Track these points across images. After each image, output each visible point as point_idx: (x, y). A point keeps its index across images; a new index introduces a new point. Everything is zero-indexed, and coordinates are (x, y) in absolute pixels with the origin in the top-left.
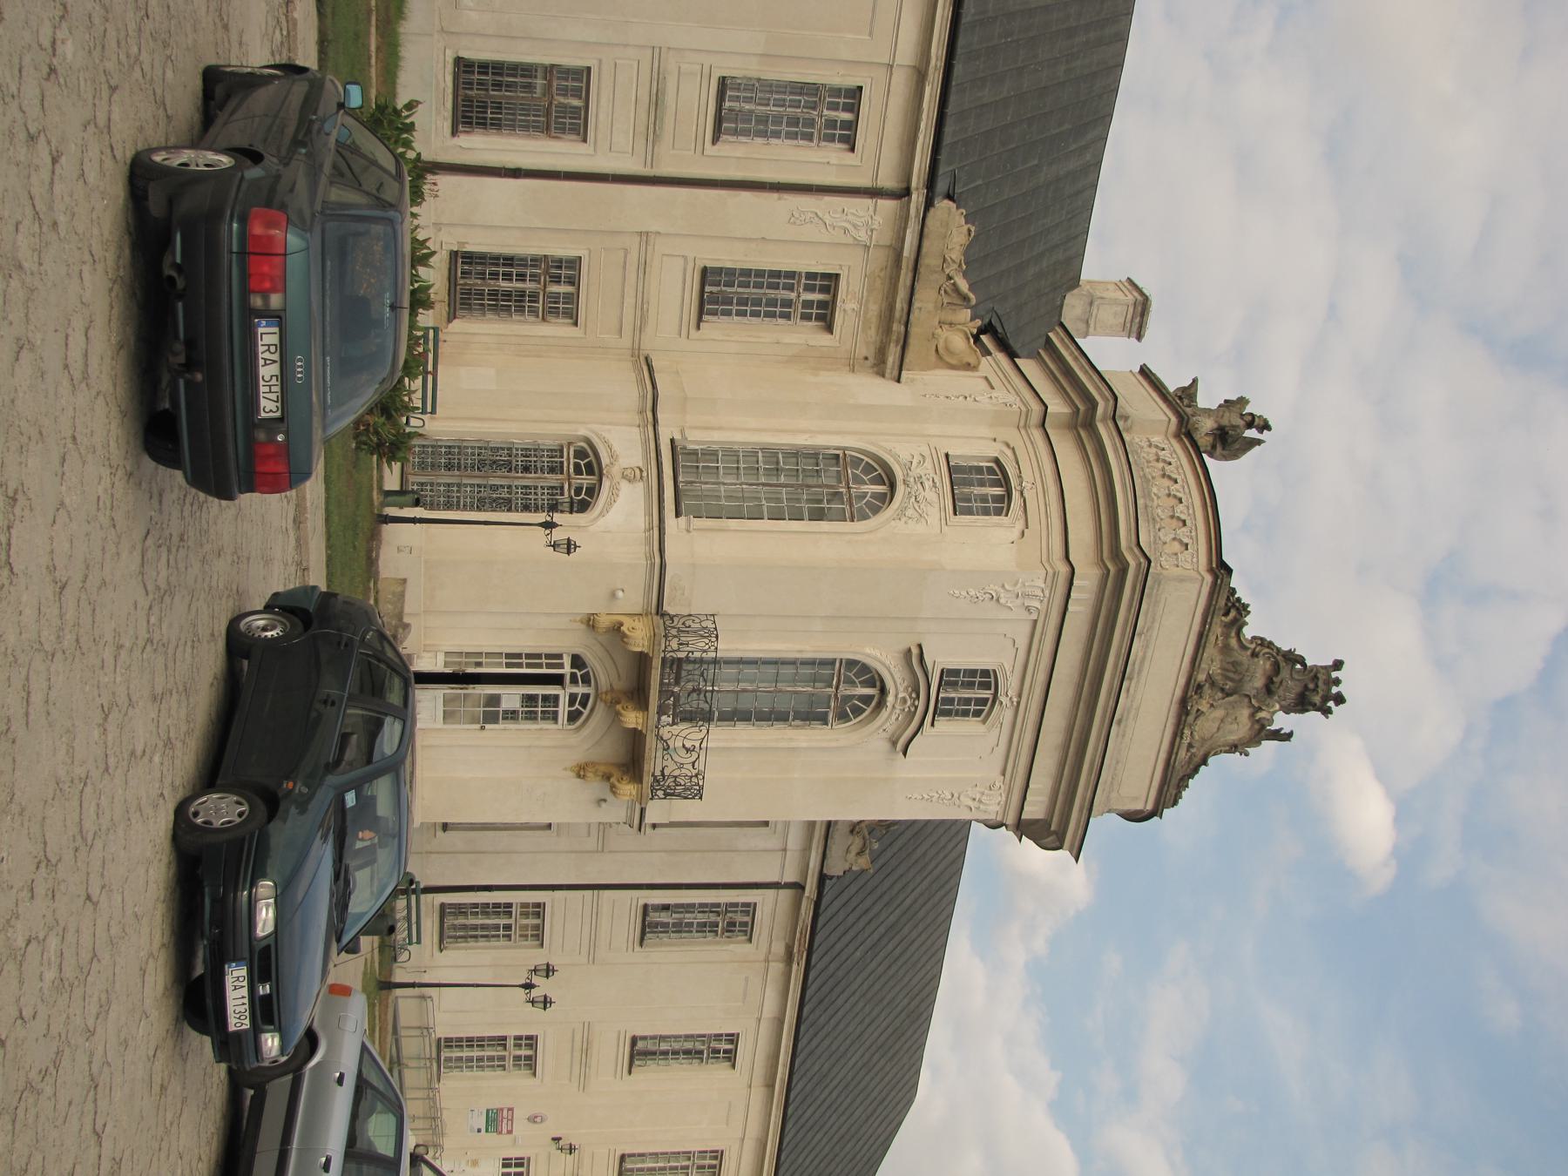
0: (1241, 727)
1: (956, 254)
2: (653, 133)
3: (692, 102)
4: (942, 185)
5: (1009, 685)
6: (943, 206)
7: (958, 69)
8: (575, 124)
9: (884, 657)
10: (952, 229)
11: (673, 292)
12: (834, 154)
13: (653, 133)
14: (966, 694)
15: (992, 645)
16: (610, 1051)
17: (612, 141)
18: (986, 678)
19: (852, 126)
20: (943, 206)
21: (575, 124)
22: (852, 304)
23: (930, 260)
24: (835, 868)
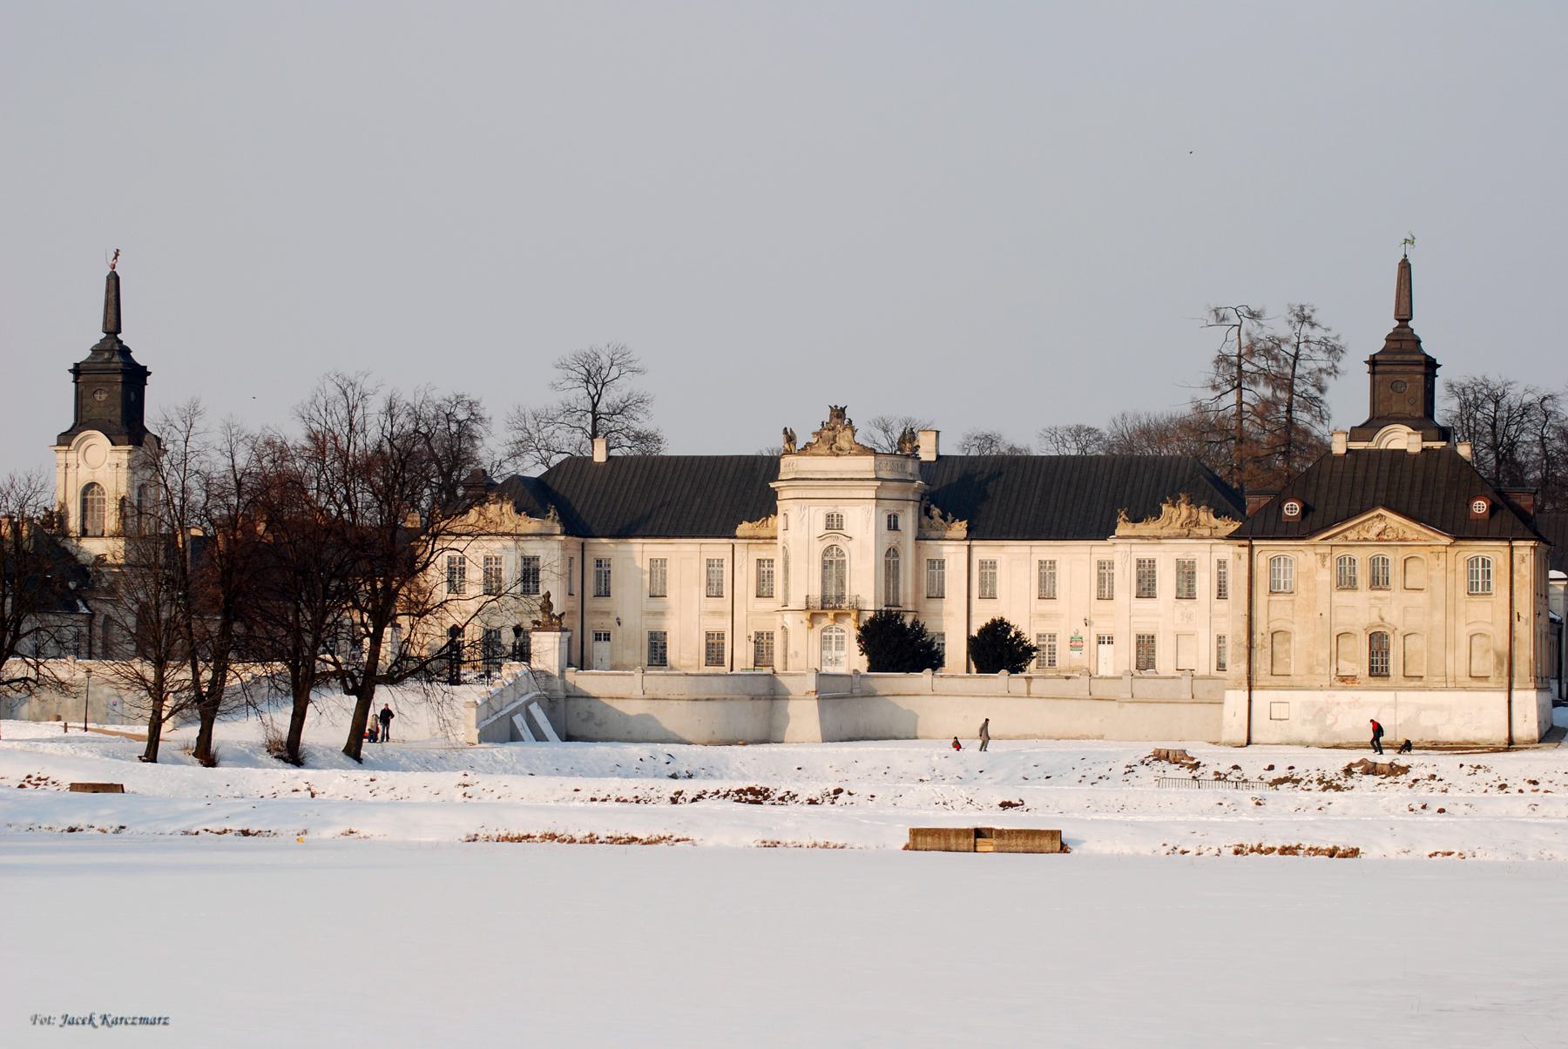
0: (848, 432)
3: (714, 603)
5: (830, 510)
6: (738, 532)
8: (721, 636)
9: (819, 547)
10: (744, 528)
11: (765, 605)
14: (834, 523)
15: (817, 516)
16: (1047, 606)
17: (723, 625)
18: (829, 517)
21: (721, 636)
22: (764, 554)
23: (751, 533)
24: (965, 533)
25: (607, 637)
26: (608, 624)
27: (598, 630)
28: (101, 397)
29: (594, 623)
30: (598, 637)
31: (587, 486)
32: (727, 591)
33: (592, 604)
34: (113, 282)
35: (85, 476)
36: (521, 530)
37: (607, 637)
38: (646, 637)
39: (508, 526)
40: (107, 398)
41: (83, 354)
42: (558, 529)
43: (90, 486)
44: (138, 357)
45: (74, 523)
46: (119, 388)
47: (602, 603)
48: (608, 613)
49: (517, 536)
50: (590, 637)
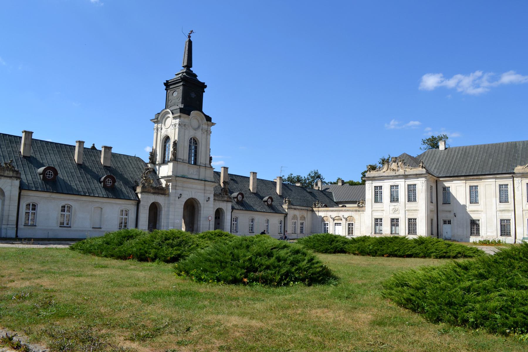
1: (522, 167)
2: (509, 211)
3: (503, 206)
4: (512, 172)
7: (495, 173)
10: (518, 169)
12: (509, 186)
13: (509, 211)
17: (510, 216)
19: (505, 185)
20: (515, 171)
25: (449, 222)
26: (450, 216)
27: (445, 219)
28: (175, 94)
29: (443, 216)
30: (445, 222)
31: (437, 159)
32: (511, 199)
33: (441, 207)
34: (187, 43)
35: (164, 132)
36: (406, 173)
37: (449, 222)
38: (469, 222)
39: (401, 172)
40: (177, 94)
41: (172, 76)
42: (424, 171)
43: (167, 139)
44: (201, 78)
45: (159, 159)
46: (181, 88)
47: (447, 207)
48: (450, 211)
49: (406, 177)
50: (441, 222)
